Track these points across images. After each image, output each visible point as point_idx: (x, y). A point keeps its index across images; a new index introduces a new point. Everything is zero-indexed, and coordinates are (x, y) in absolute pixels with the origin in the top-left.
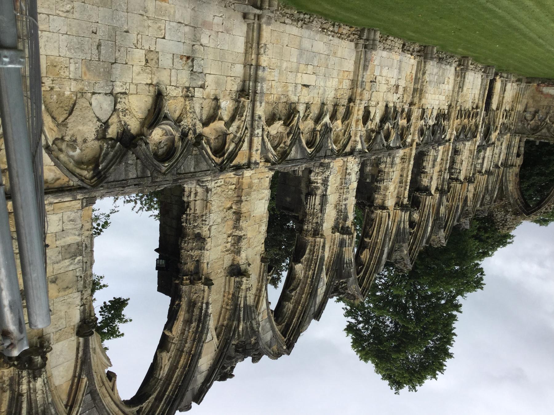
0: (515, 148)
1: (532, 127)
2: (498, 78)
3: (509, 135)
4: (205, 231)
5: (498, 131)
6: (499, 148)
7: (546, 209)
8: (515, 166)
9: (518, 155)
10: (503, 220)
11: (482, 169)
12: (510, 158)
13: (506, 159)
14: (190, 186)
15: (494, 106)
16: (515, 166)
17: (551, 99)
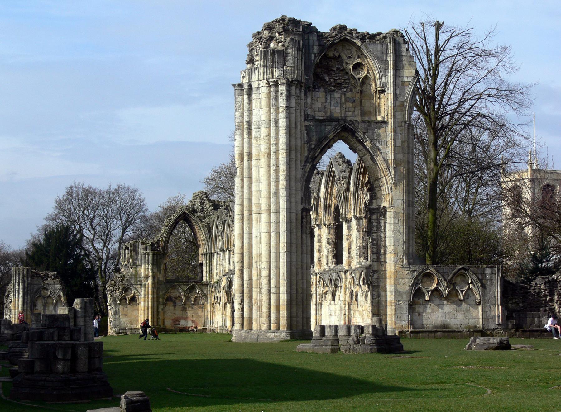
0: (205, 271)
1: (194, 291)
2: (230, 329)
3: (212, 282)
4: (328, 245)
5: (222, 285)
6: (219, 270)
7: (170, 220)
8: (202, 255)
9: (201, 264)
10: (204, 203)
11: (229, 253)
12: (207, 261)
13: (210, 260)
14: (332, 266)
15: (229, 306)
16: (202, 255)
17: (184, 316)
